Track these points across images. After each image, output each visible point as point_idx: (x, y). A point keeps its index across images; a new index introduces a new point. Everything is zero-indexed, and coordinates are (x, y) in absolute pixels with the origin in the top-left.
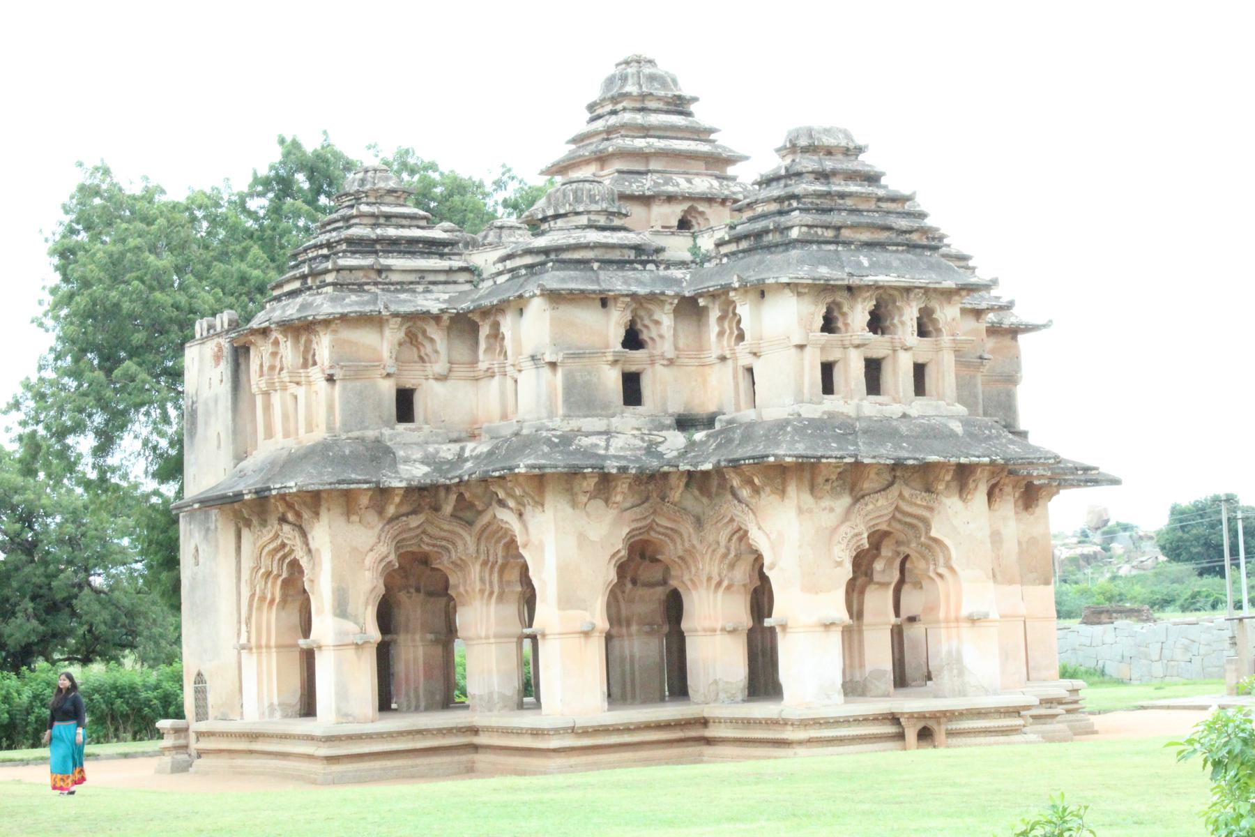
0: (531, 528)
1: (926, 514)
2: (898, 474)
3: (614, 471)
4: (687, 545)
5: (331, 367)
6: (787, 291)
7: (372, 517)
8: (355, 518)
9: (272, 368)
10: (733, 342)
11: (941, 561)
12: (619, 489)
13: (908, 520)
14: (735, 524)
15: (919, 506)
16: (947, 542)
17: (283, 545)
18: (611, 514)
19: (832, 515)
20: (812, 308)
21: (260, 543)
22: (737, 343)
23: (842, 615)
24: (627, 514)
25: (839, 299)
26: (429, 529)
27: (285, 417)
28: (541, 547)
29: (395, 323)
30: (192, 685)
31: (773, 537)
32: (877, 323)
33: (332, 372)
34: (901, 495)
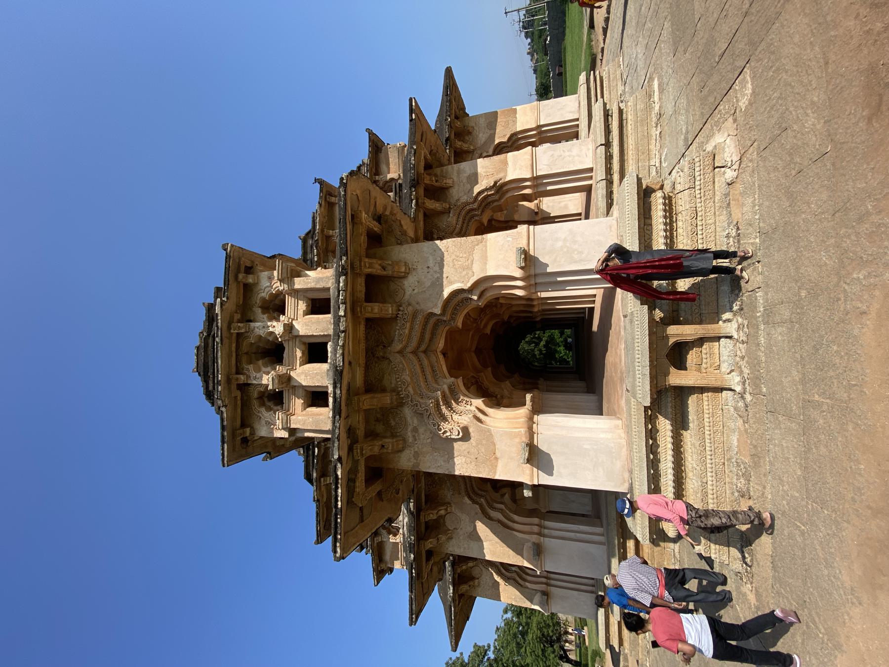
1: (420, 318)
2: (381, 354)
3: (412, 556)
7: (476, 572)
11: (465, 295)
12: (435, 517)
13: (427, 336)
15: (411, 329)
16: (446, 294)
18: (453, 509)
19: (421, 430)
20: (263, 422)
23: (522, 412)
25: (256, 395)
29: (378, 539)
32: (274, 352)
34: (400, 352)
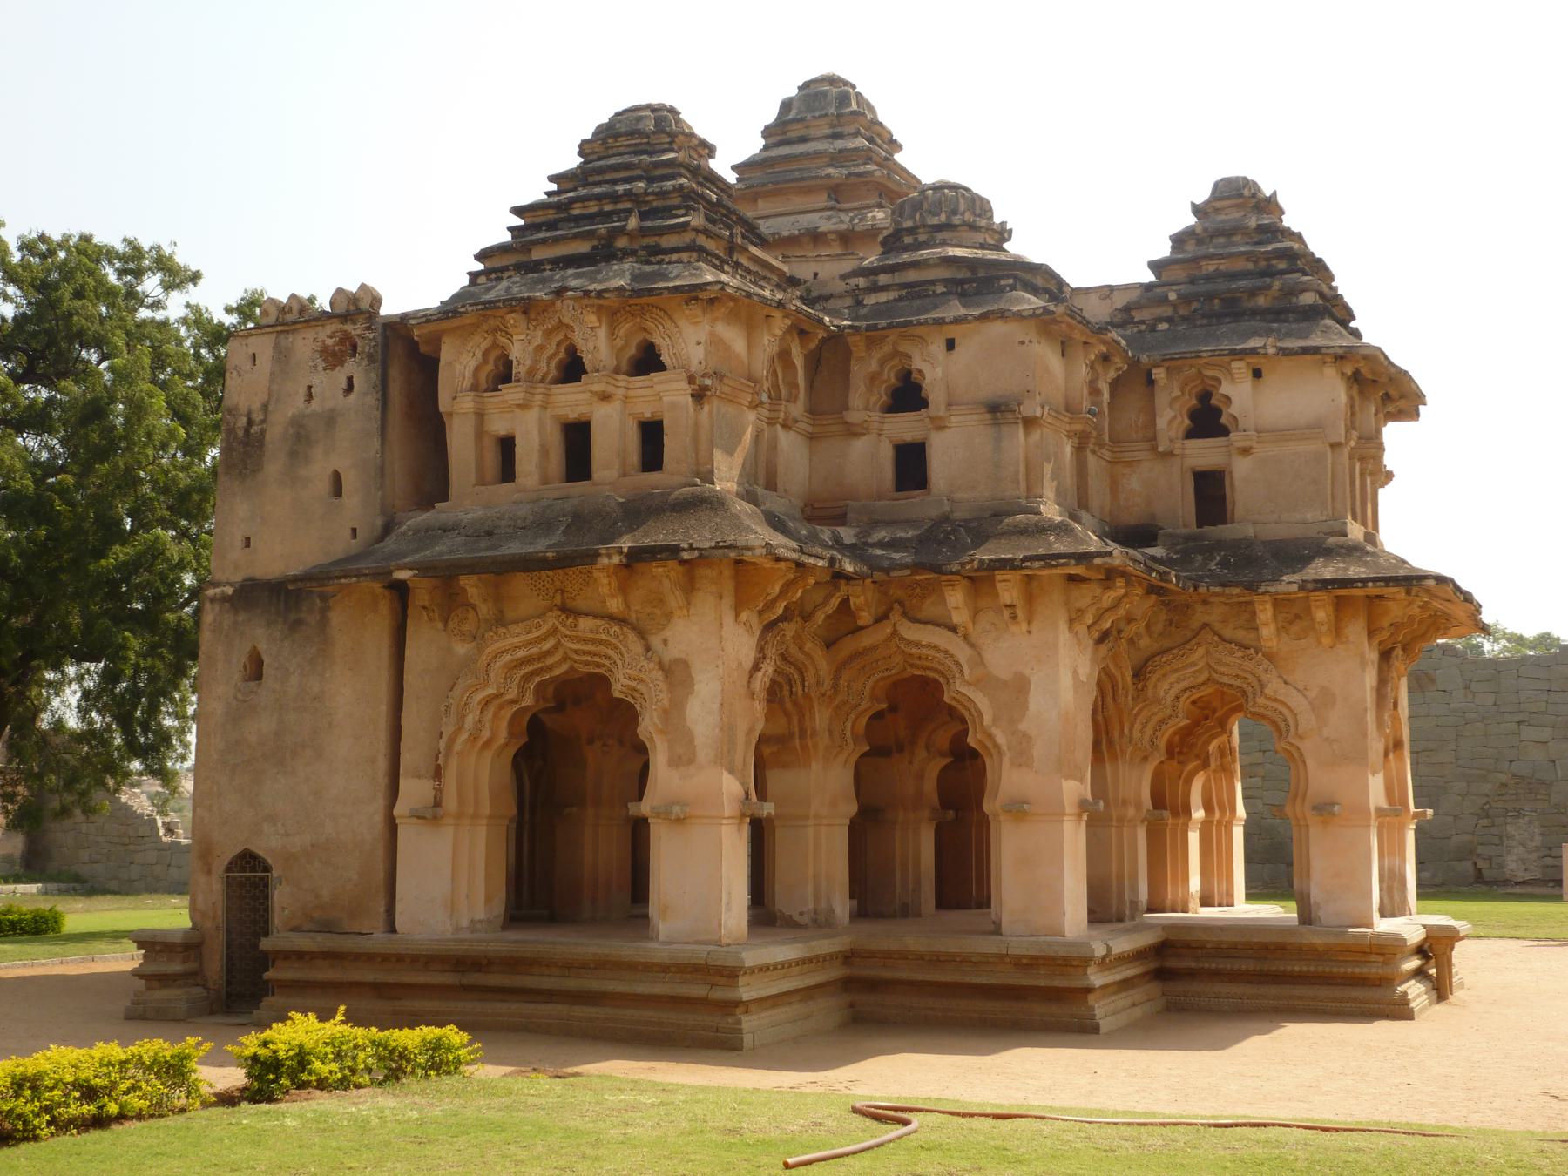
0: (988, 656)
4: (1121, 700)
5: (705, 375)
6: (1330, 372)
7: (754, 620)
8: (744, 616)
9: (531, 372)
10: (1181, 434)
14: (1205, 676)
17: (549, 653)
21: (500, 645)
22: (1191, 434)
24: (1103, 649)
26: (793, 650)
27: (544, 452)
28: (1021, 686)
30: (222, 869)
31: (1313, 694)
33: (708, 382)
